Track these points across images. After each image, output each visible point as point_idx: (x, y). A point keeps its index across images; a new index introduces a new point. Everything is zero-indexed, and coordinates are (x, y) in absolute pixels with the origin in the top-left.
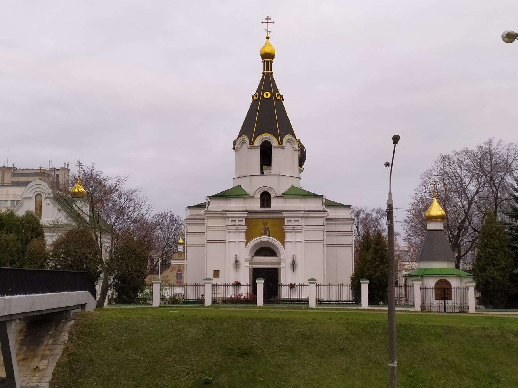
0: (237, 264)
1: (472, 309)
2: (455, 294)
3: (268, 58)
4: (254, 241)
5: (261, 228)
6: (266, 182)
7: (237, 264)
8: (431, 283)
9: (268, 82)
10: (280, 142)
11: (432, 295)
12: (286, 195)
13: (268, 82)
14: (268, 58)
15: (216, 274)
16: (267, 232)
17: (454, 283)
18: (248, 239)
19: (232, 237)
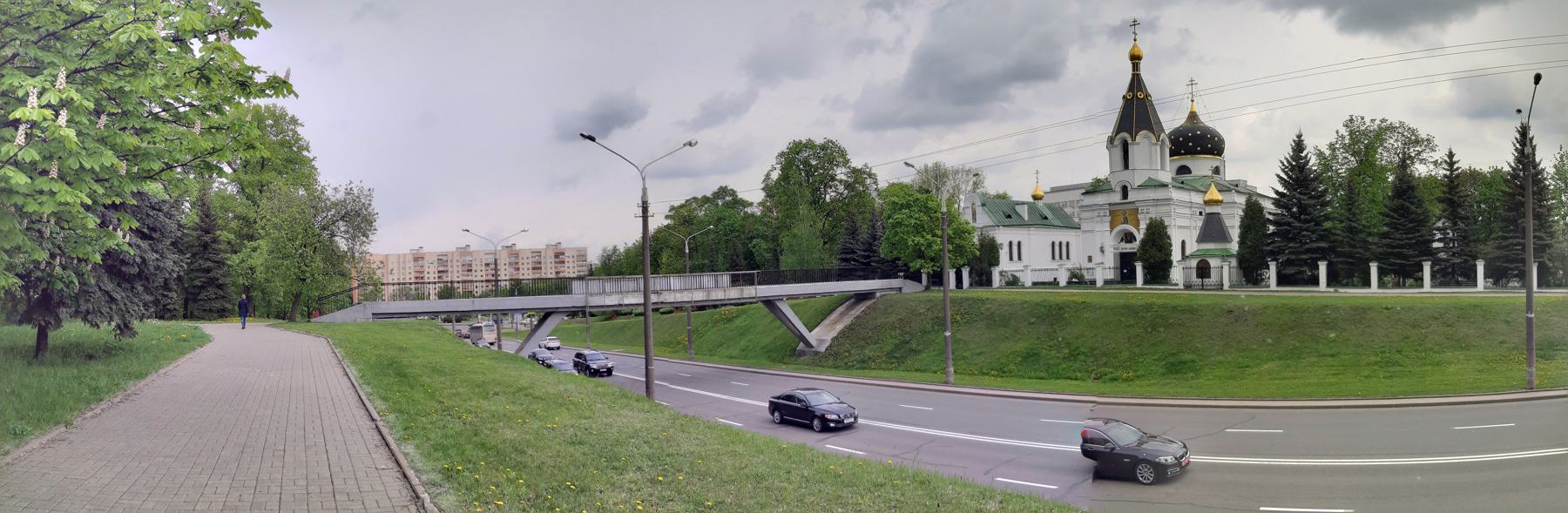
0: (1102, 250)
1: (1226, 287)
2: (1213, 273)
3: (1135, 59)
4: (1117, 229)
5: (1121, 218)
6: (1125, 176)
7: (1102, 250)
8: (1194, 263)
9: (1136, 83)
10: (1134, 139)
11: (1194, 273)
12: (1141, 187)
13: (1136, 83)
14: (1135, 59)
15: (1090, 259)
16: (1126, 221)
17: (1214, 263)
18: (1112, 228)
19: (1098, 227)
